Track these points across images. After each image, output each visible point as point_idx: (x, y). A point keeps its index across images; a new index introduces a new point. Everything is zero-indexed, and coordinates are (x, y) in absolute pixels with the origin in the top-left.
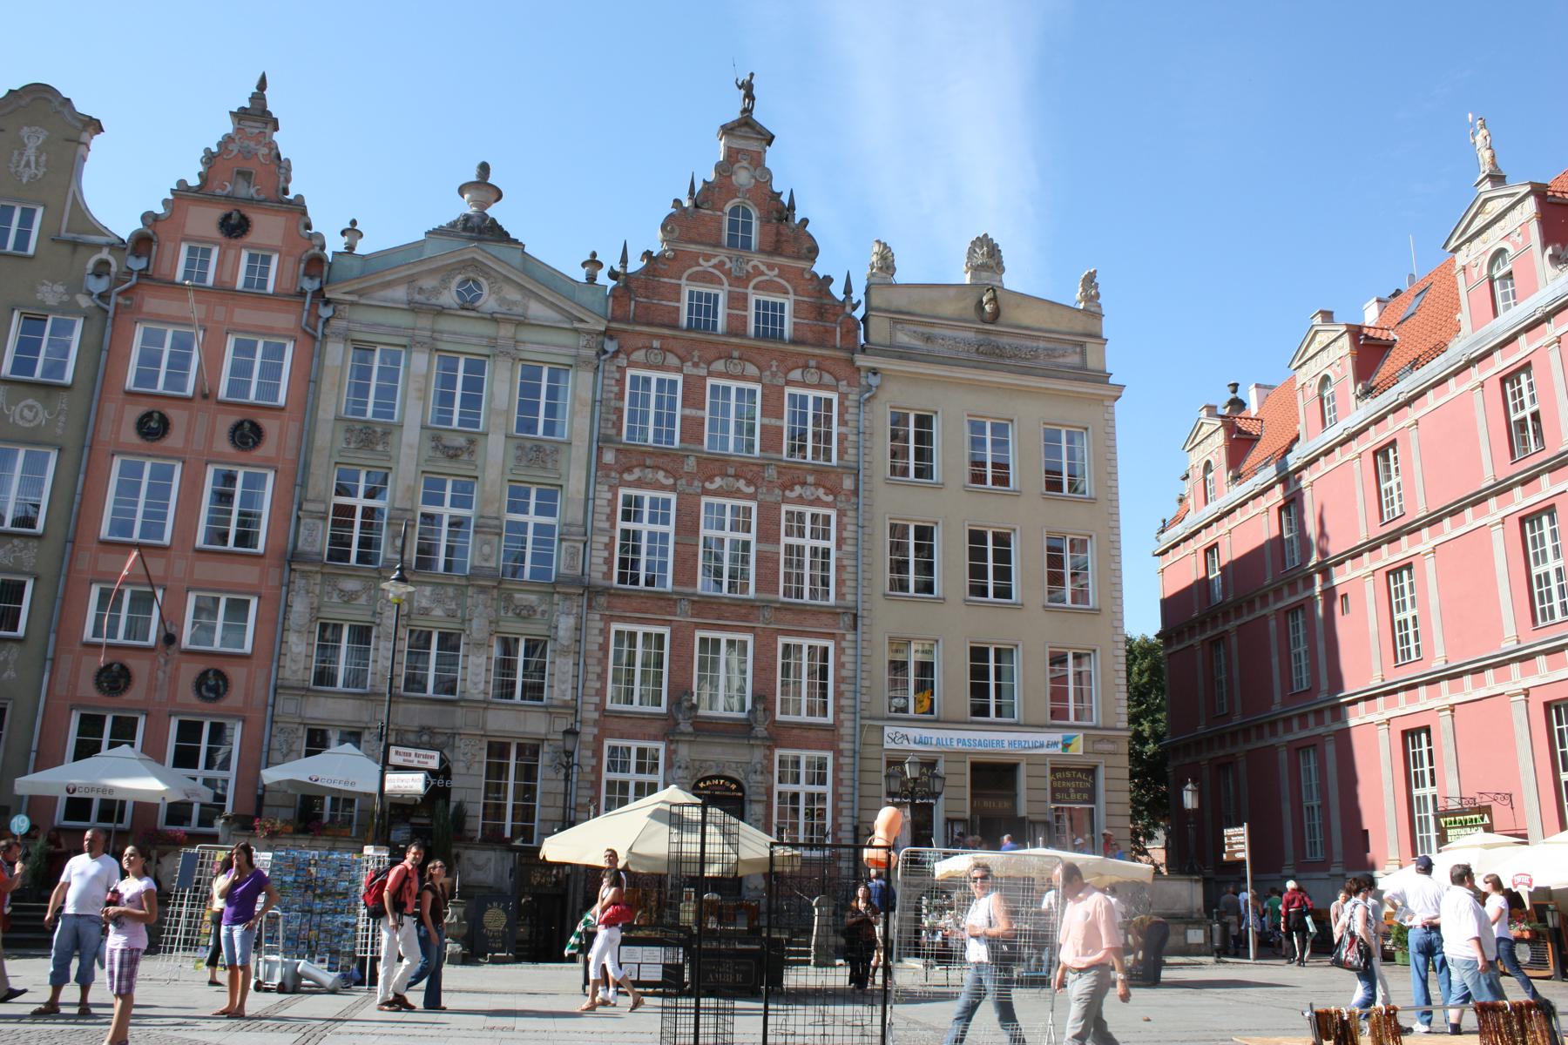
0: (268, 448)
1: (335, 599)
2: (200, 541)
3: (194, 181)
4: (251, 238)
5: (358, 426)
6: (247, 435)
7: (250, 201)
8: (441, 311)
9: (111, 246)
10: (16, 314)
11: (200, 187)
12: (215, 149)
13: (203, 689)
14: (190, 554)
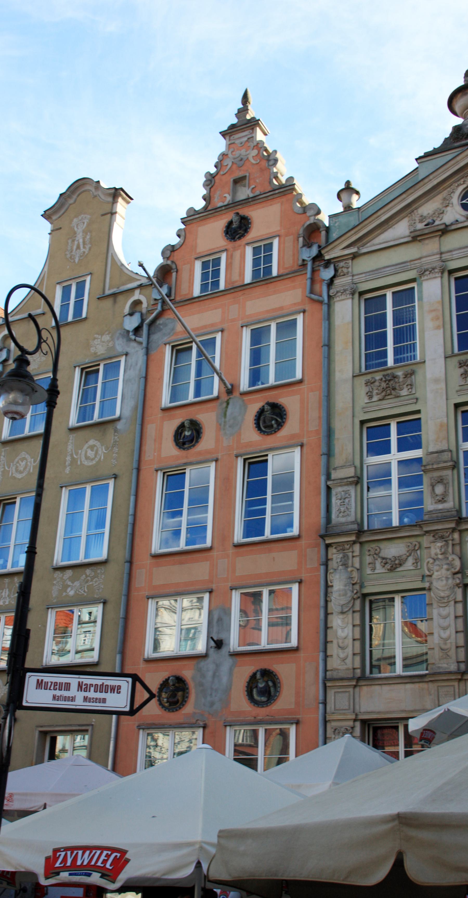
0: (291, 426)
1: (379, 569)
2: (238, 536)
3: (199, 204)
4: (253, 234)
5: (378, 377)
6: (271, 418)
7: (247, 201)
8: (445, 231)
9: (140, 286)
10: (78, 371)
11: (205, 208)
12: (213, 170)
13: (255, 691)
14: (231, 551)
